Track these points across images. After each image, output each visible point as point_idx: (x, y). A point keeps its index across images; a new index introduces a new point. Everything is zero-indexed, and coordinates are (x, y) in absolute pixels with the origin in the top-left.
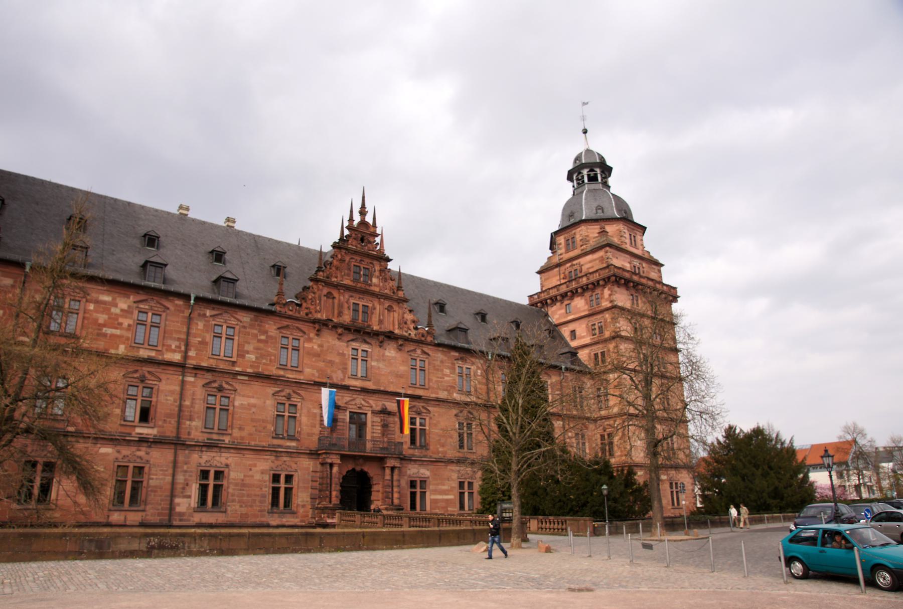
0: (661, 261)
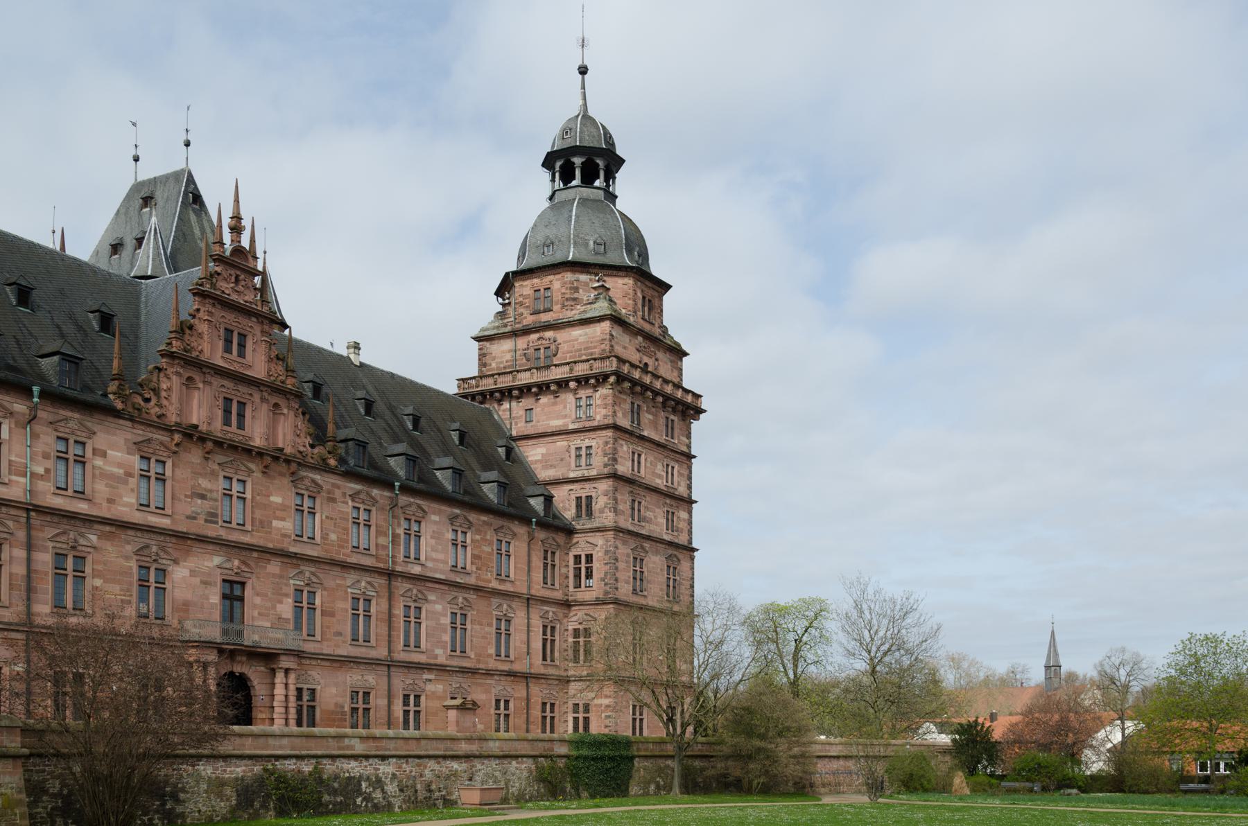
0: (685, 347)
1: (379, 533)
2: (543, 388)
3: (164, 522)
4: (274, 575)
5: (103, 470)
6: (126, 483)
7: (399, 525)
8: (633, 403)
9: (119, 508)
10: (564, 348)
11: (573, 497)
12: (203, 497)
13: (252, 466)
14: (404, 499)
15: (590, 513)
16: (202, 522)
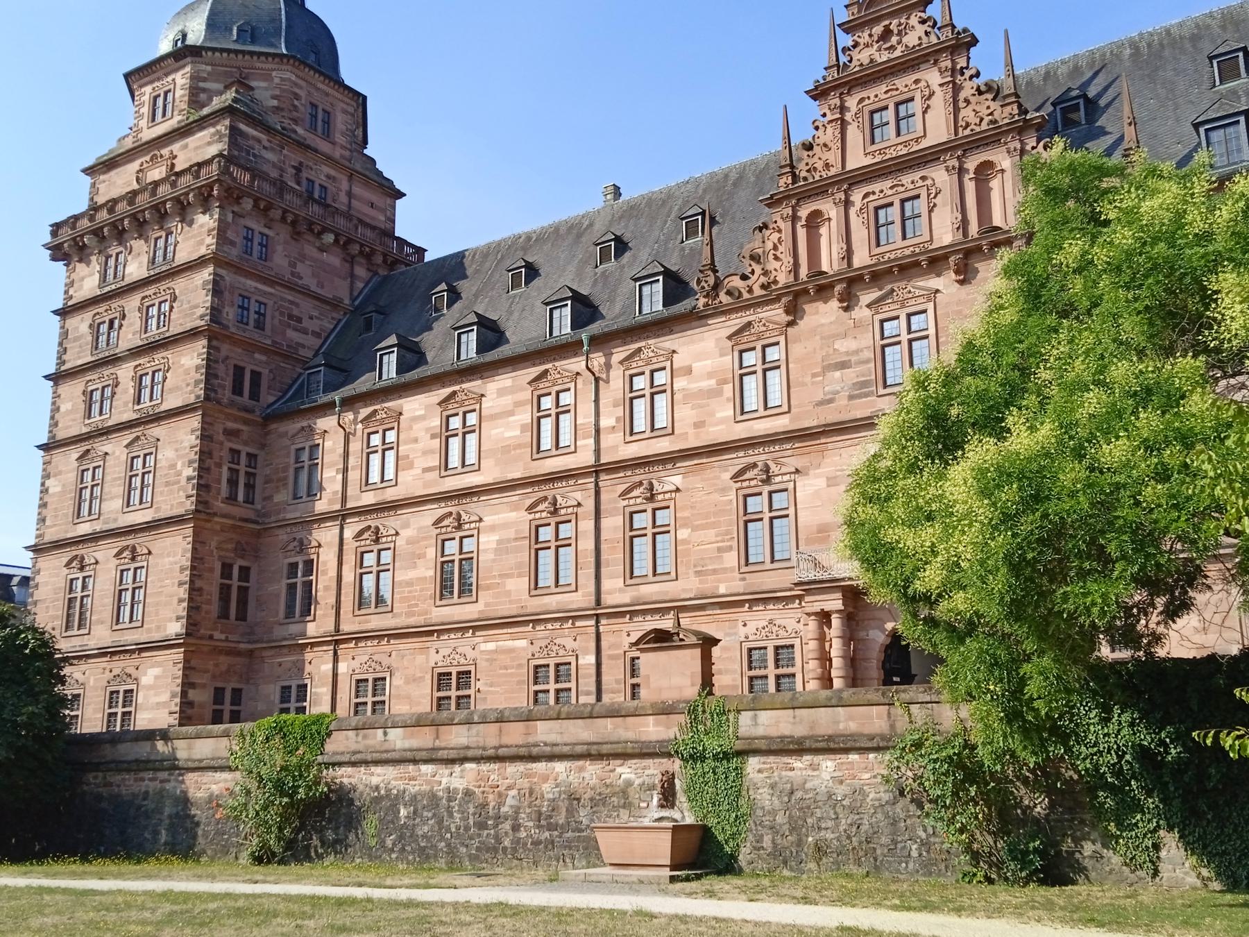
3: (782, 424)
5: (687, 390)
9: (711, 429)
12: (843, 365)
13: (934, 282)
16: (844, 402)
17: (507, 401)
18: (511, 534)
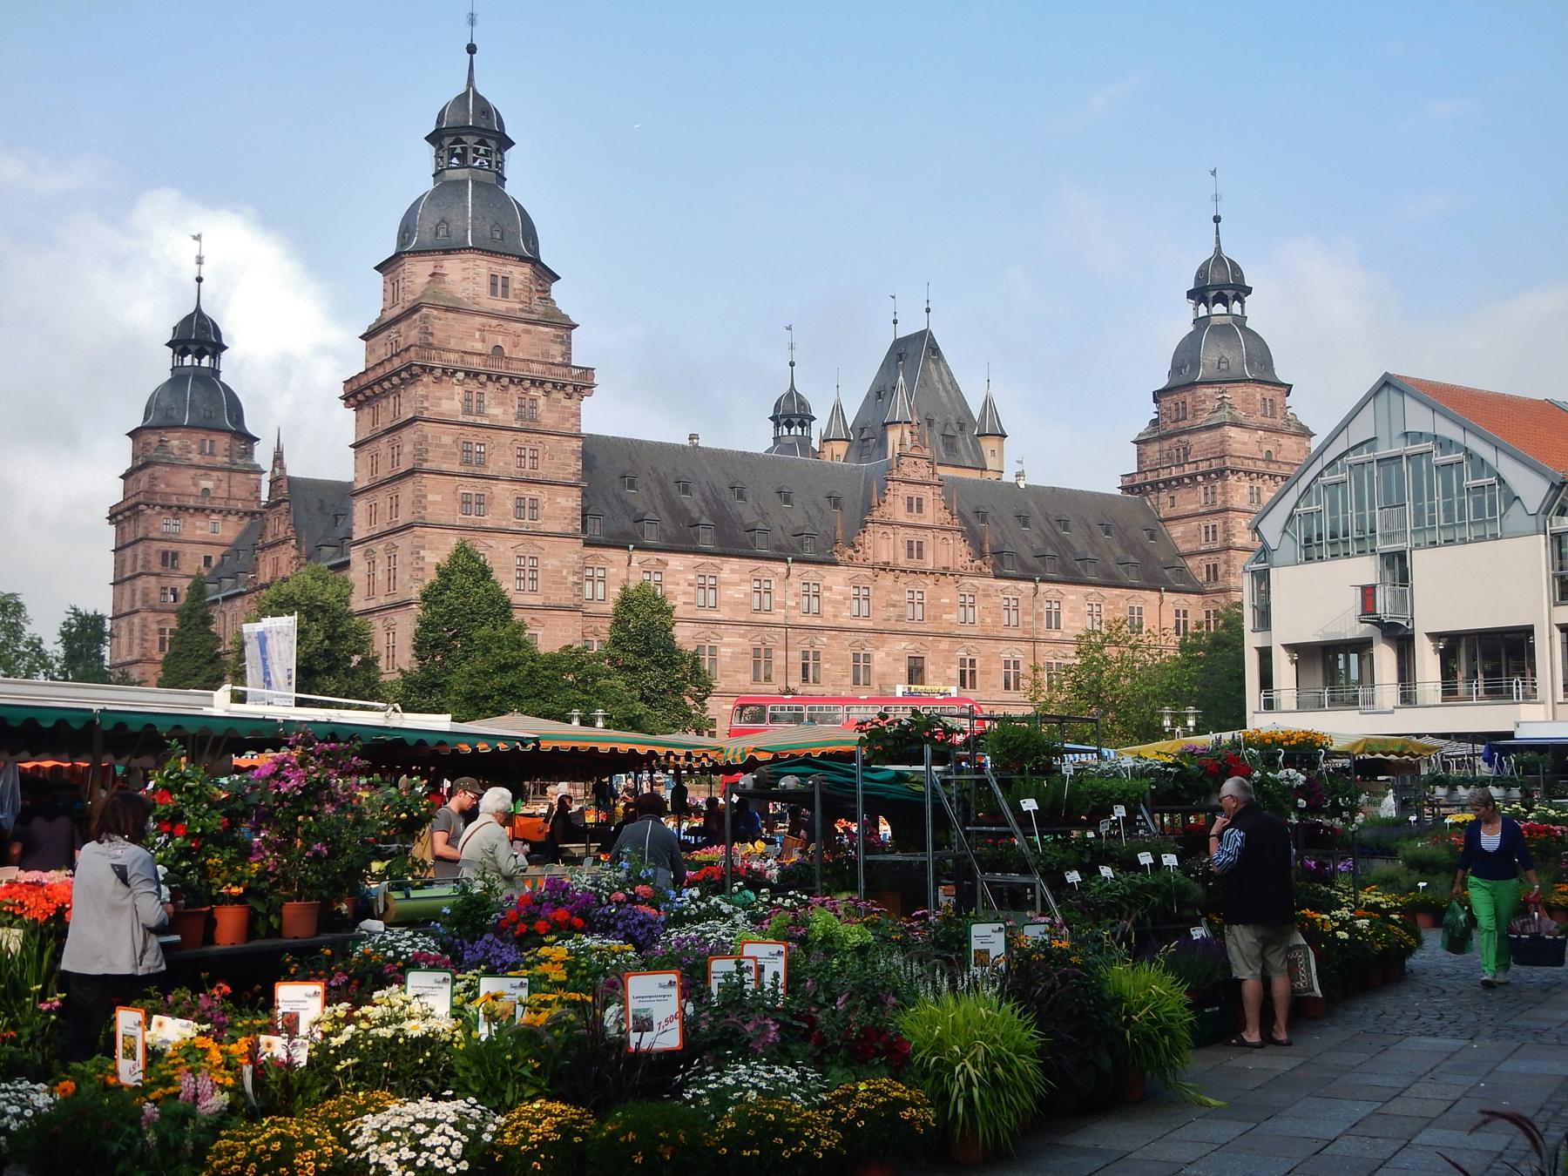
1: (1025, 614)
2: (1180, 480)
3: (869, 624)
4: (945, 651)
6: (844, 604)
7: (1041, 606)
8: (1252, 487)
10: (1196, 448)
11: (1204, 565)
12: (894, 606)
14: (1043, 587)
15: (1216, 579)
17: (736, 577)
18: (739, 649)
